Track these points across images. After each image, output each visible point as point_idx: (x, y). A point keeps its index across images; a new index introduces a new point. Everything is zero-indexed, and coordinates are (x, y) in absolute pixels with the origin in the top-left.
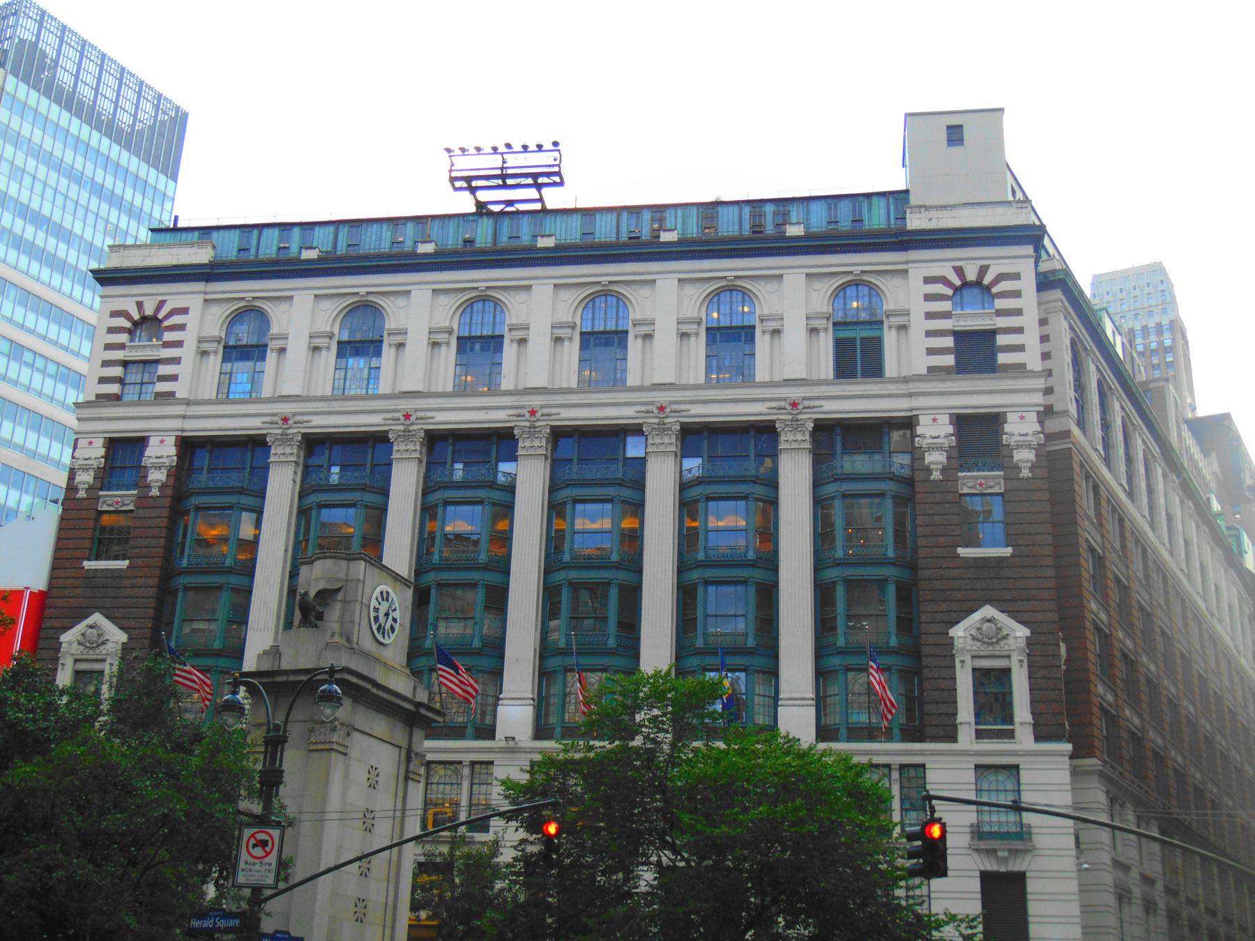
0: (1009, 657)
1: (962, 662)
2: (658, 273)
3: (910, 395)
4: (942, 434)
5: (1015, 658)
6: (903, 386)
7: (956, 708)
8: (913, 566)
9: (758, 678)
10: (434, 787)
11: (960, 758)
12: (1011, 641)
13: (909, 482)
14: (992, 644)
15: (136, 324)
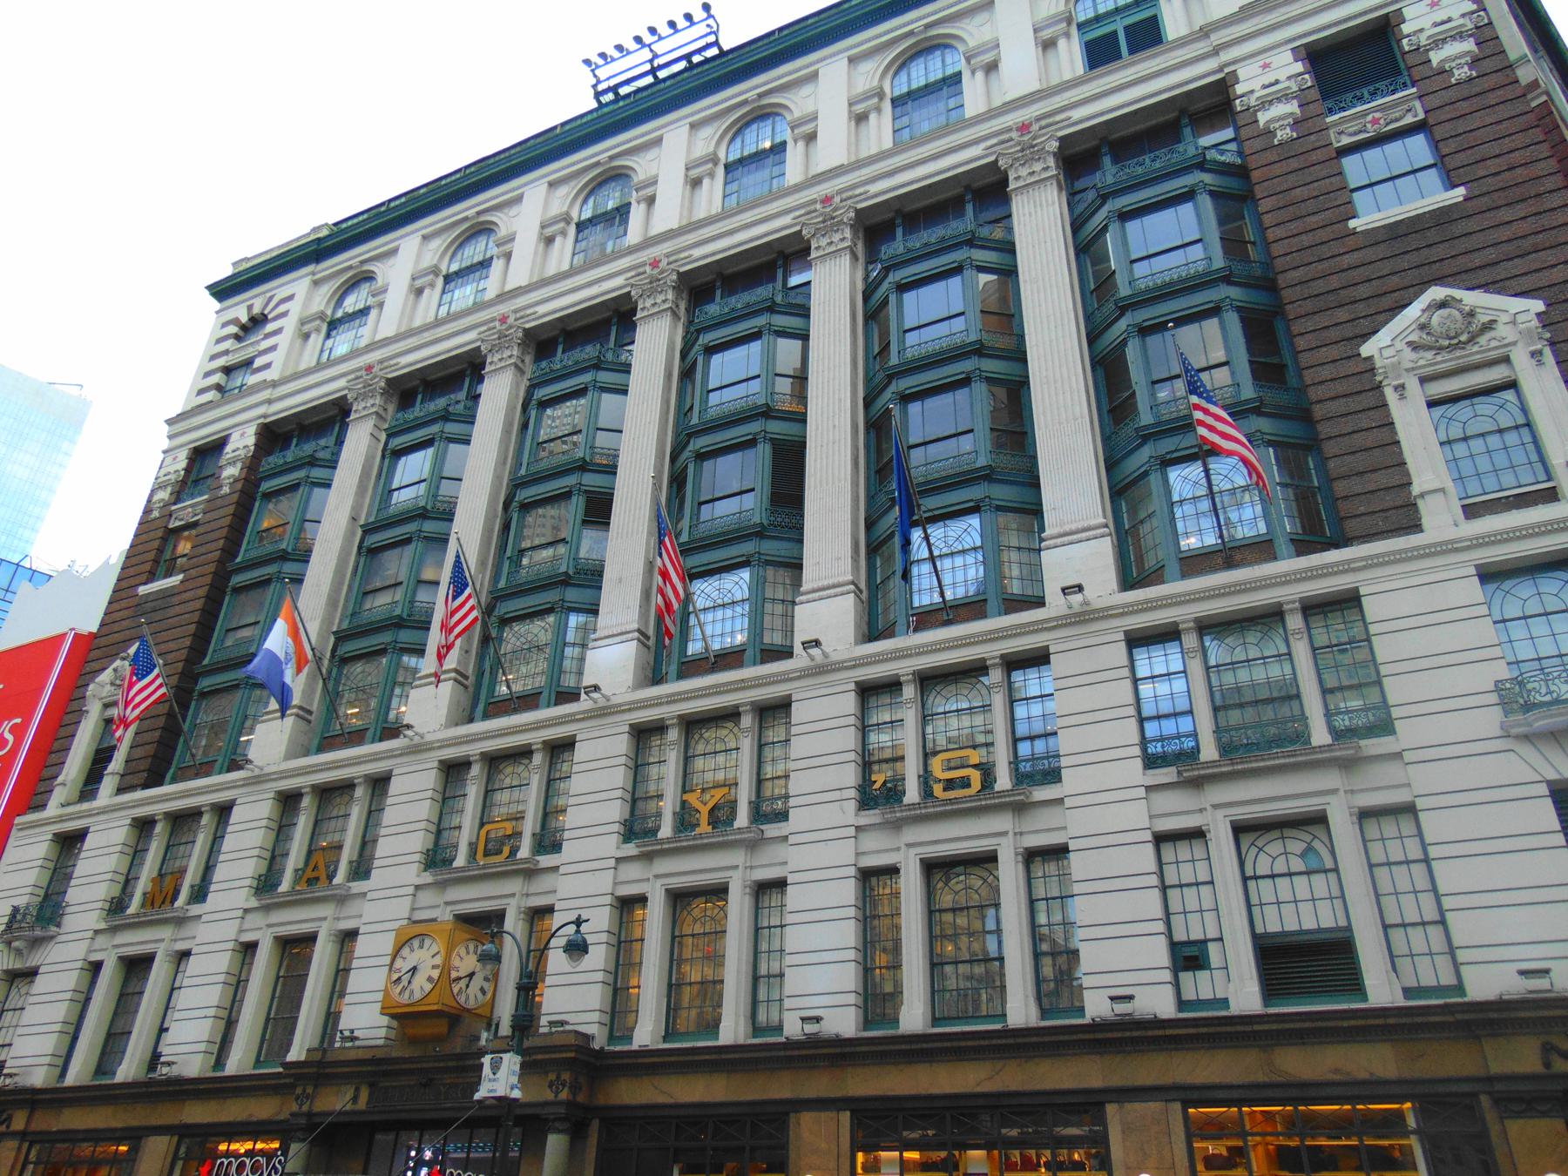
0: (1506, 360)
1: (1400, 388)
2: (818, 61)
3: (1216, 52)
4: (1282, 77)
5: (1520, 357)
6: (1201, 44)
7: (1408, 474)
8: (1268, 284)
9: (1010, 520)
10: (948, 969)
11: (1439, 561)
12: (1504, 331)
13: (1240, 172)
14: (1461, 345)
15: (244, 328)
